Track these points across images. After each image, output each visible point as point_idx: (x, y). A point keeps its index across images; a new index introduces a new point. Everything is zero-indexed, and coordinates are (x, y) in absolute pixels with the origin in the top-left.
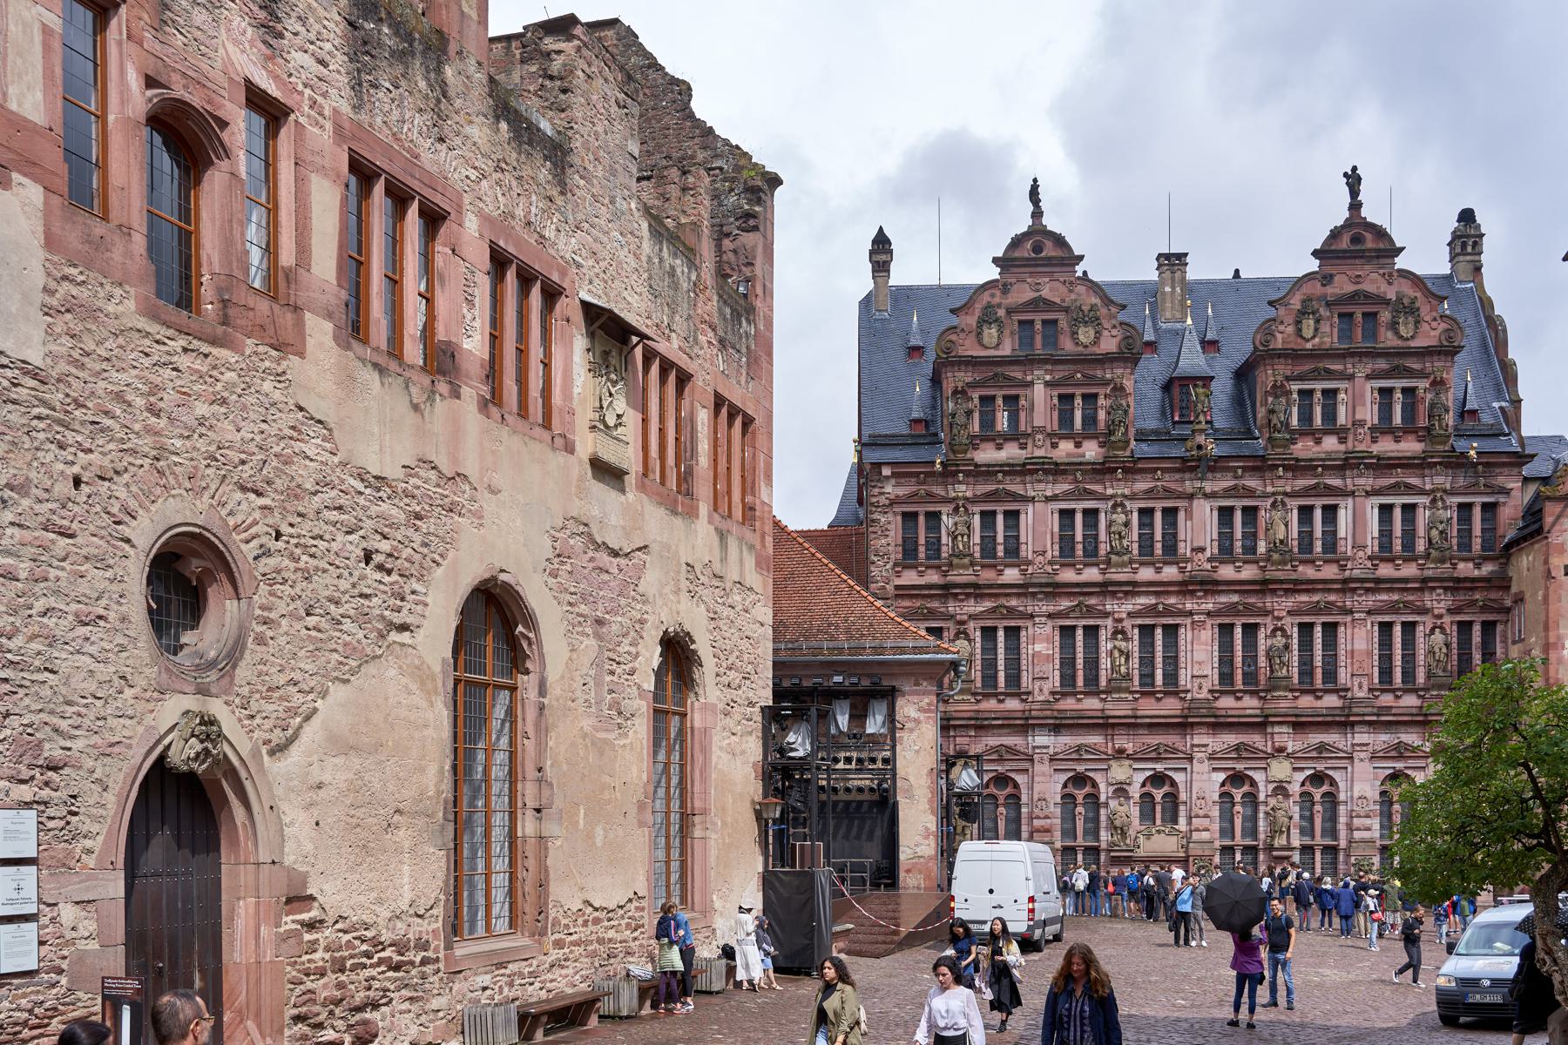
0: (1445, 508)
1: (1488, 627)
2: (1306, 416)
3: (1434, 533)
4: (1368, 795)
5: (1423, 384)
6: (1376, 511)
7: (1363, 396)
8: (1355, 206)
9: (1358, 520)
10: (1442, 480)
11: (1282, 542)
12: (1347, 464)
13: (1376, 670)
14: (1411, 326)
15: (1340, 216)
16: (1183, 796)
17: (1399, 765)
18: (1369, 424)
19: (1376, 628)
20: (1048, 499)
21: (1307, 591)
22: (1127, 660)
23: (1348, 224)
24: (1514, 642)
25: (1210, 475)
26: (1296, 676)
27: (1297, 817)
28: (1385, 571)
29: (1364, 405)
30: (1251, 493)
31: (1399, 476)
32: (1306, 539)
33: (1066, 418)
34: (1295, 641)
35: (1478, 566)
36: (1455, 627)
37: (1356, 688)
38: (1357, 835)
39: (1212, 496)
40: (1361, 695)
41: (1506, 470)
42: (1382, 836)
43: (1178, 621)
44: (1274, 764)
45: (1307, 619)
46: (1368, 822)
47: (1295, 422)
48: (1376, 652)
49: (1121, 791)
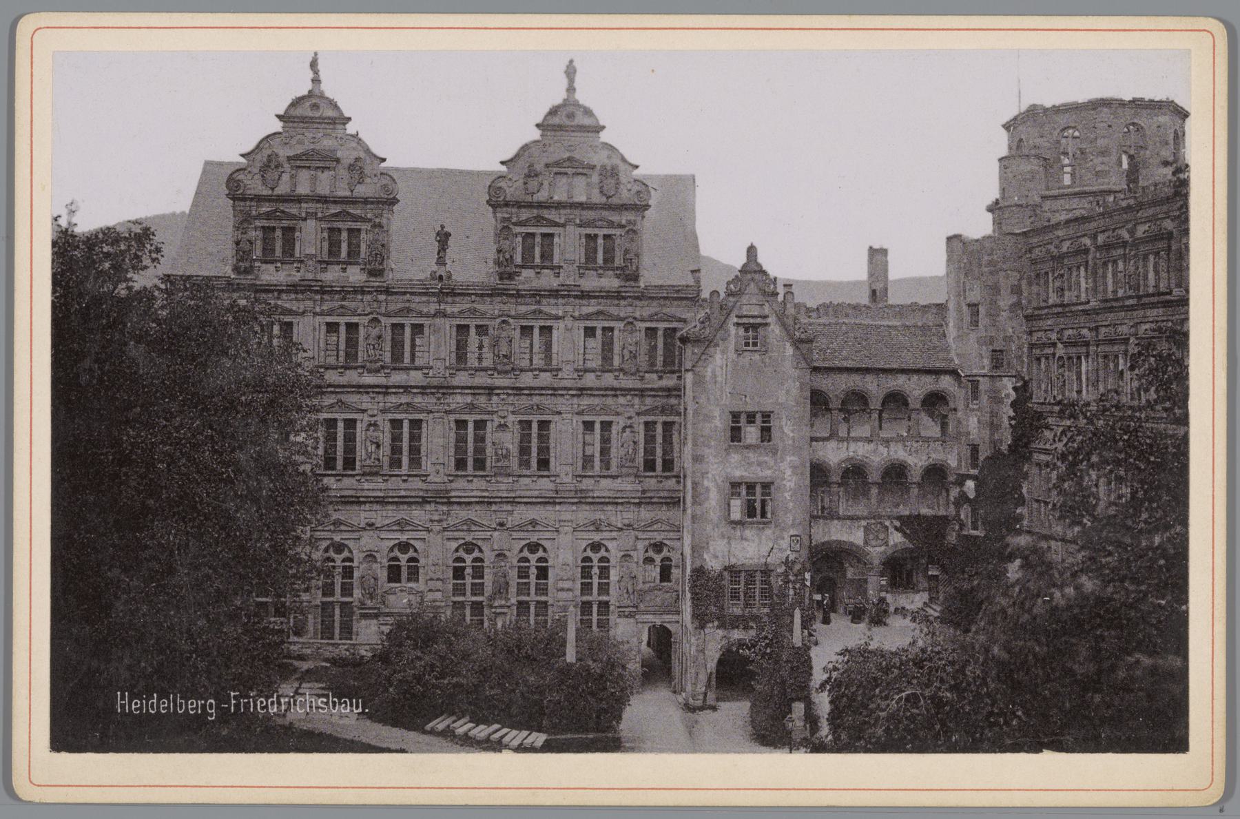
1: (668, 426)
2: (528, 251)
3: (626, 352)
4: (570, 562)
8: (571, 89)
15: (558, 97)
16: (422, 561)
20: (315, 314)
22: (378, 446)
23: (565, 103)
25: (450, 299)
30: (483, 315)
33: (334, 246)
35: (660, 378)
37: (562, 475)
39: (453, 316)
43: (420, 416)
44: (496, 534)
47: (518, 259)
49: (371, 557)
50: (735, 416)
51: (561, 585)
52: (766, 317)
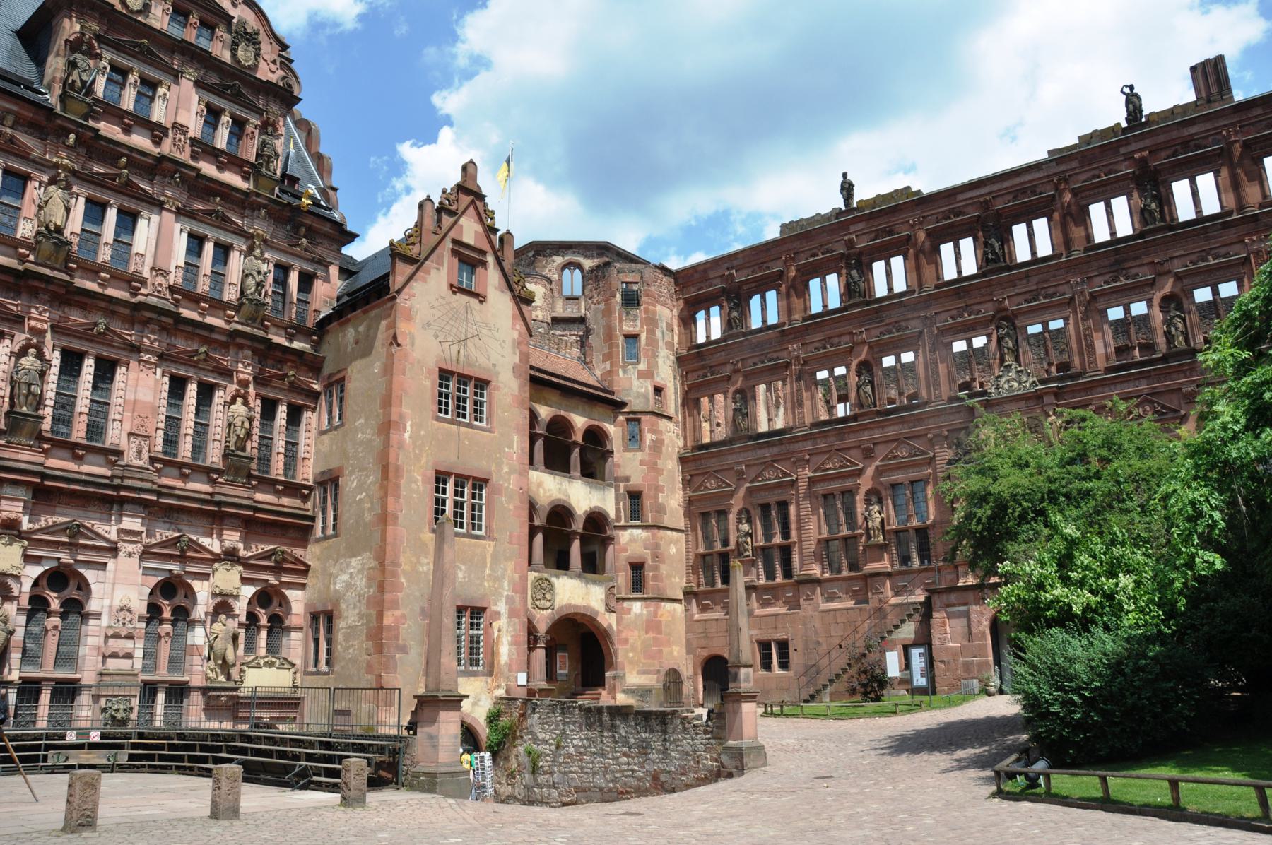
0: (264, 261)
5: (255, 121)
6: (185, 236)
7: (189, 99)
9: (162, 239)
10: (260, 227)
11: (59, 230)
12: (159, 167)
13: (161, 433)
14: (251, 55)
17: (176, 568)
18: (191, 134)
19: (166, 379)
21: (83, 307)
24: (325, 432)
26: (48, 420)
27: (20, 632)
28: (186, 313)
29: (189, 111)
30: (24, 156)
31: (217, 204)
32: (90, 238)
34: (55, 370)
35: (291, 338)
36: (259, 402)
38: (113, 664)
40: (137, 462)
41: (326, 242)
42: (144, 669)
45: (77, 345)
46: (128, 645)
48: (163, 410)
50: (445, 375)
51: (114, 645)
52: (484, 253)
